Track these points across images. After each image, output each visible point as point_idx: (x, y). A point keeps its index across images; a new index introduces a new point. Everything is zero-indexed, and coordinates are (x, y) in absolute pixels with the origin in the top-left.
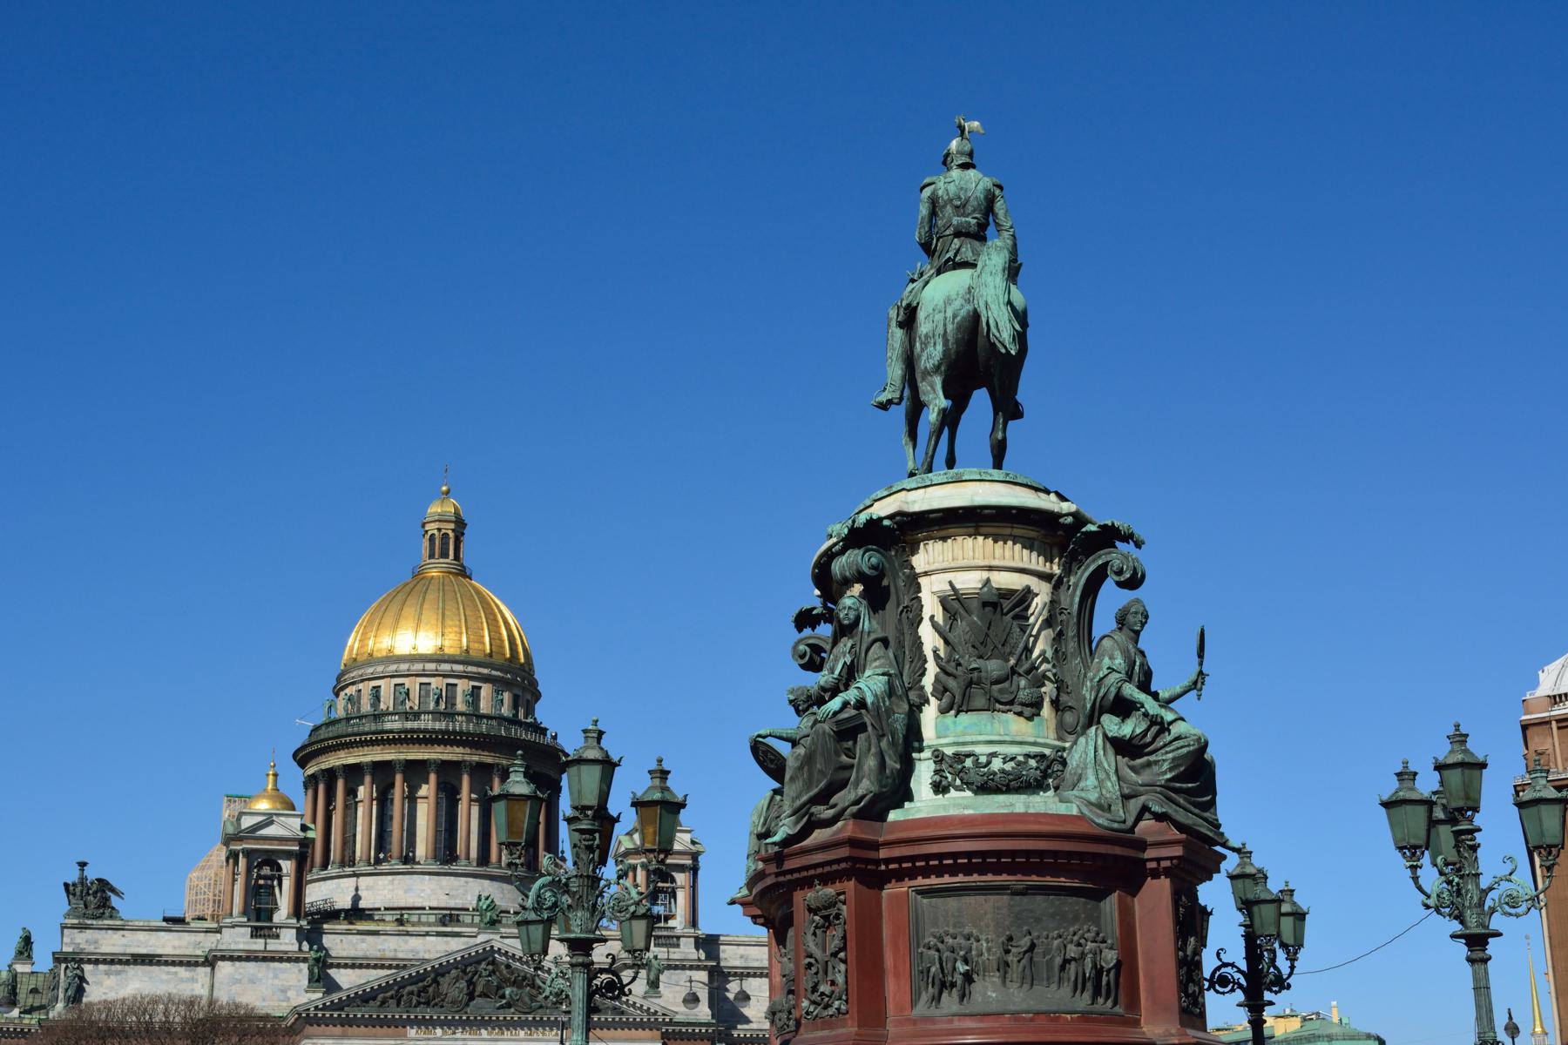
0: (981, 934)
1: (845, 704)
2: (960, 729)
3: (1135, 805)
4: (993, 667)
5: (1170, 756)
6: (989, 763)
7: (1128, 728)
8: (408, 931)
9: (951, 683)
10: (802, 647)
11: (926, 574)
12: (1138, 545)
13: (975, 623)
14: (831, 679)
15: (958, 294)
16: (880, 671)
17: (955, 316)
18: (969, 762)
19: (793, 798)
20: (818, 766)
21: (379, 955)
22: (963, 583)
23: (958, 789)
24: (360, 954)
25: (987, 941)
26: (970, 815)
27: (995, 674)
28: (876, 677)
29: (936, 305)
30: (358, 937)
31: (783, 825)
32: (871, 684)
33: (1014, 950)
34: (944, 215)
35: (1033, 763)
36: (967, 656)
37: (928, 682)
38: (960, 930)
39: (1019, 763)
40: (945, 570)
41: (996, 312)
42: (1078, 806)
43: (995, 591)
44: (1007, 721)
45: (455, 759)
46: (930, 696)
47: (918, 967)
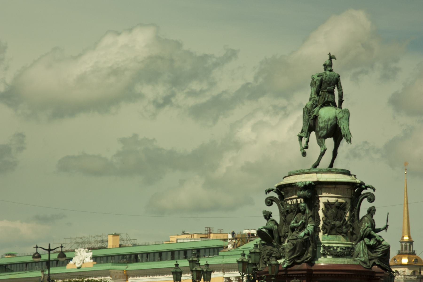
1: (305, 234)
2: (329, 239)
3: (372, 262)
4: (338, 223)
5: (381, 250)
7: (372, 242)
9: (327, 227)
10: (268, 200)
12: (374, 190)
13: (333, 211)
15: (332, 118)
16: (312, 225)
17: (331, 124)
22: (331, 200)
23: (329, 255)
26: (334, 264)
27: (338, 225)
28: (311, 226)
29: (326, 120)
32: (310, 228)
34: (324, 85)
37: (320, 226)
39: (344, 249)
41: (346, 131)
43: (339, 203)
44: (340, 238)
46: (321, 230)
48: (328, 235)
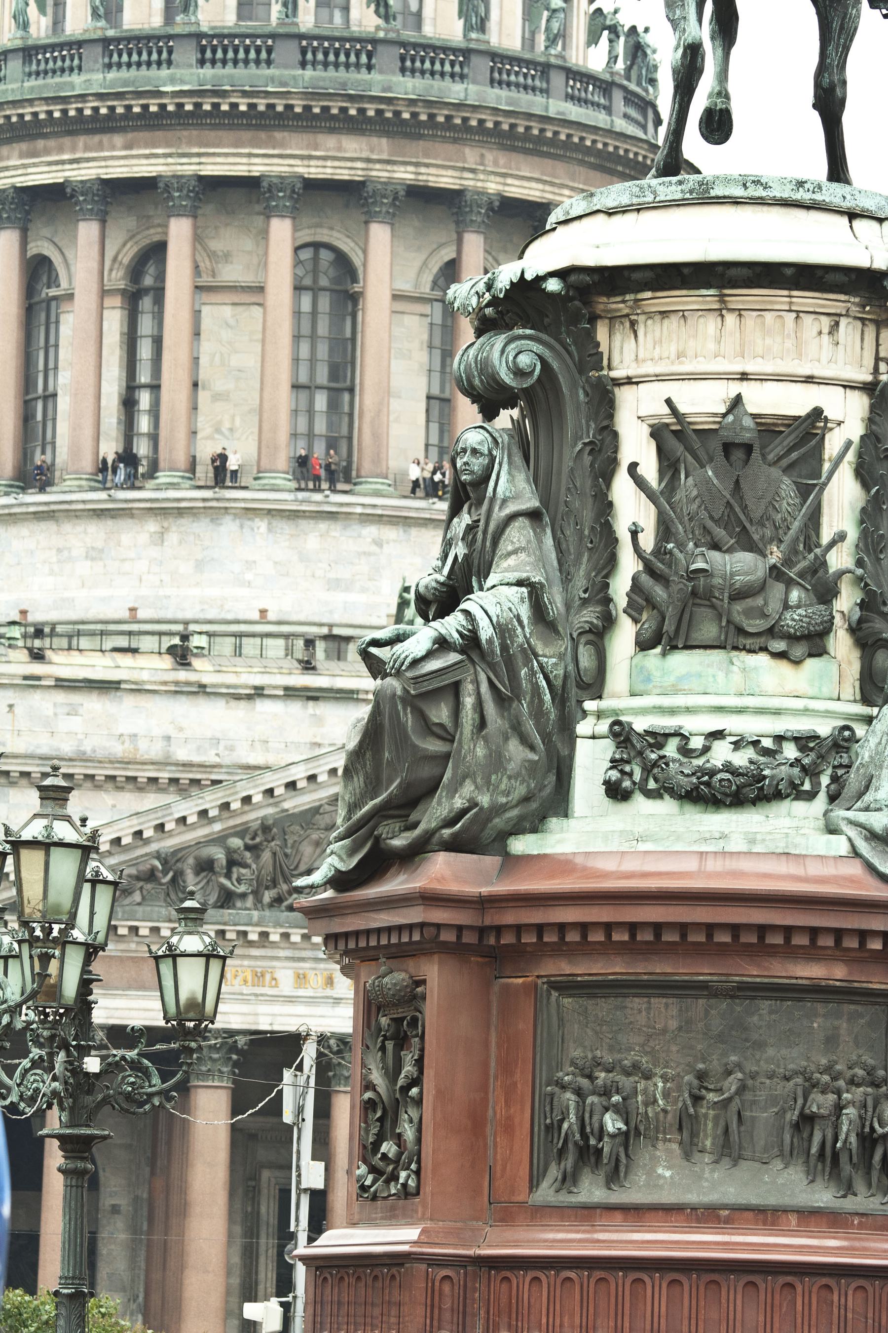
0: (655, 1066)
1: (442, 644)
6: (706, 749)
8: (203, 686)
9: (659, 592)
11: (629, 381)
13: (708, 480)
14: (434, 584)
16: (513, 577)
18: (671, 749)
19: (349, 806)
20: (387, 754)
21: (119, 750)
24: (67, 748)
25: (665, 1078)
30: (61, 697)
31: (332, 853)
33: (712, 1097)
35: (790, 751)
36: (691, 545)
38: (618, 1056)
40: (659, 378)
42: (850, 840)
45: (344, 175)
47: (546, 1118)
48: (664, 654)
